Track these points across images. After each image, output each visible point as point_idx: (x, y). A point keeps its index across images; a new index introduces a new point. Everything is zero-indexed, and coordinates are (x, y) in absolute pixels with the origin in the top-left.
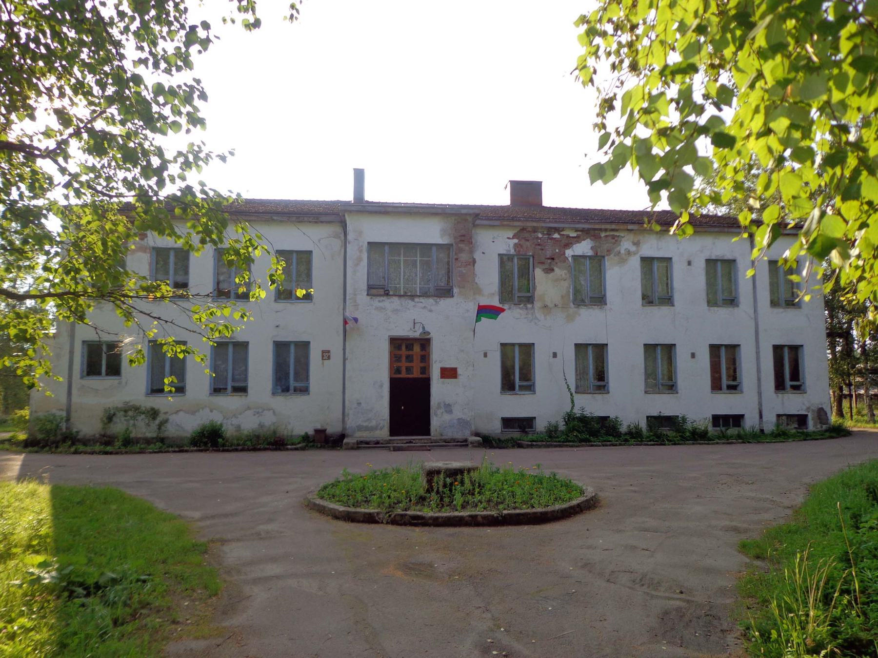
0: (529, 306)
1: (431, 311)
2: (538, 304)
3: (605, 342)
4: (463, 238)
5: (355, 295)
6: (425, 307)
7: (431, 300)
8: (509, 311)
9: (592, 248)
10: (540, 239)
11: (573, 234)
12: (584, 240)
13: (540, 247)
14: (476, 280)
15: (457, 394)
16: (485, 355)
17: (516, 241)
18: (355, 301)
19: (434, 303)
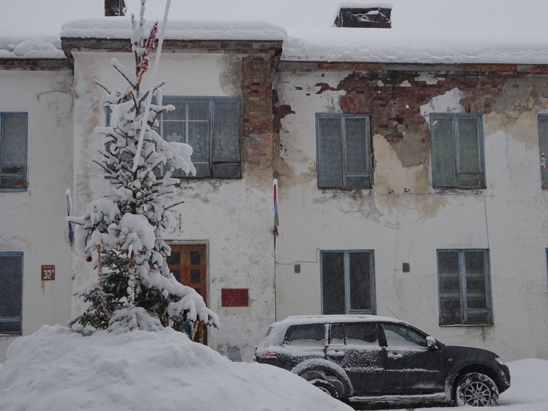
0: (365, 192)
1: (206, 201)
2: (377, 190)
3: (486, 247)
4: (255, 88)
5: (87, 177)
6: (197, 195)
7: (206, 185)
8: (334, 201)
9: (462, 102)
11: (431, 81)
12: (449, 89)
15: (248, 331)
16: (297, 269)
17: (343, 93)
18: (87, 187)
19: (211, 188)
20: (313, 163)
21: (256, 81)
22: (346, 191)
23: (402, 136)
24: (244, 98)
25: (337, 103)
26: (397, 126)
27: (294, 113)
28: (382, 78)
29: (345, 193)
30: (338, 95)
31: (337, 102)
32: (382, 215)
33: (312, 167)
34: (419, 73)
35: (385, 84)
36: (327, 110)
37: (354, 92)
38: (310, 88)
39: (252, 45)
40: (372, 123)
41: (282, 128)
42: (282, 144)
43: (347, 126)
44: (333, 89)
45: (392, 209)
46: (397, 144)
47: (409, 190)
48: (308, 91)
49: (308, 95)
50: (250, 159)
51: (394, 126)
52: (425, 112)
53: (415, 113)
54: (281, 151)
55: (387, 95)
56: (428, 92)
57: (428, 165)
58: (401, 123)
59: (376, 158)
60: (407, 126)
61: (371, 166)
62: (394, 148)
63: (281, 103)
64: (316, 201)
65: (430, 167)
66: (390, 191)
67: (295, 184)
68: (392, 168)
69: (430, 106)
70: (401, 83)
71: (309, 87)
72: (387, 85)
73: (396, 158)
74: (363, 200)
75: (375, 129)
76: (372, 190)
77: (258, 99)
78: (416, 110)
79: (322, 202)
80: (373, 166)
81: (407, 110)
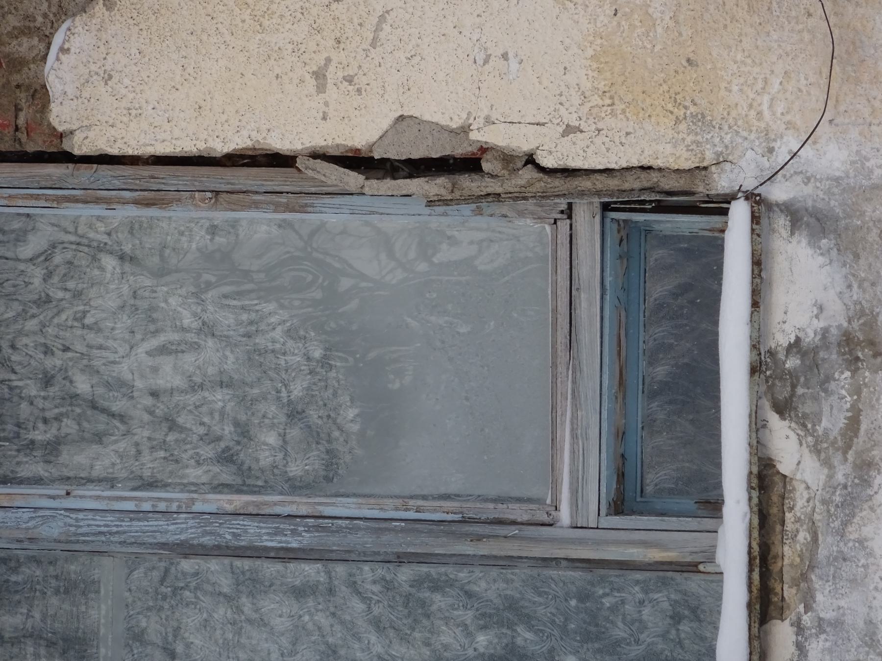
61: (469, 183)
76: (778, 193)
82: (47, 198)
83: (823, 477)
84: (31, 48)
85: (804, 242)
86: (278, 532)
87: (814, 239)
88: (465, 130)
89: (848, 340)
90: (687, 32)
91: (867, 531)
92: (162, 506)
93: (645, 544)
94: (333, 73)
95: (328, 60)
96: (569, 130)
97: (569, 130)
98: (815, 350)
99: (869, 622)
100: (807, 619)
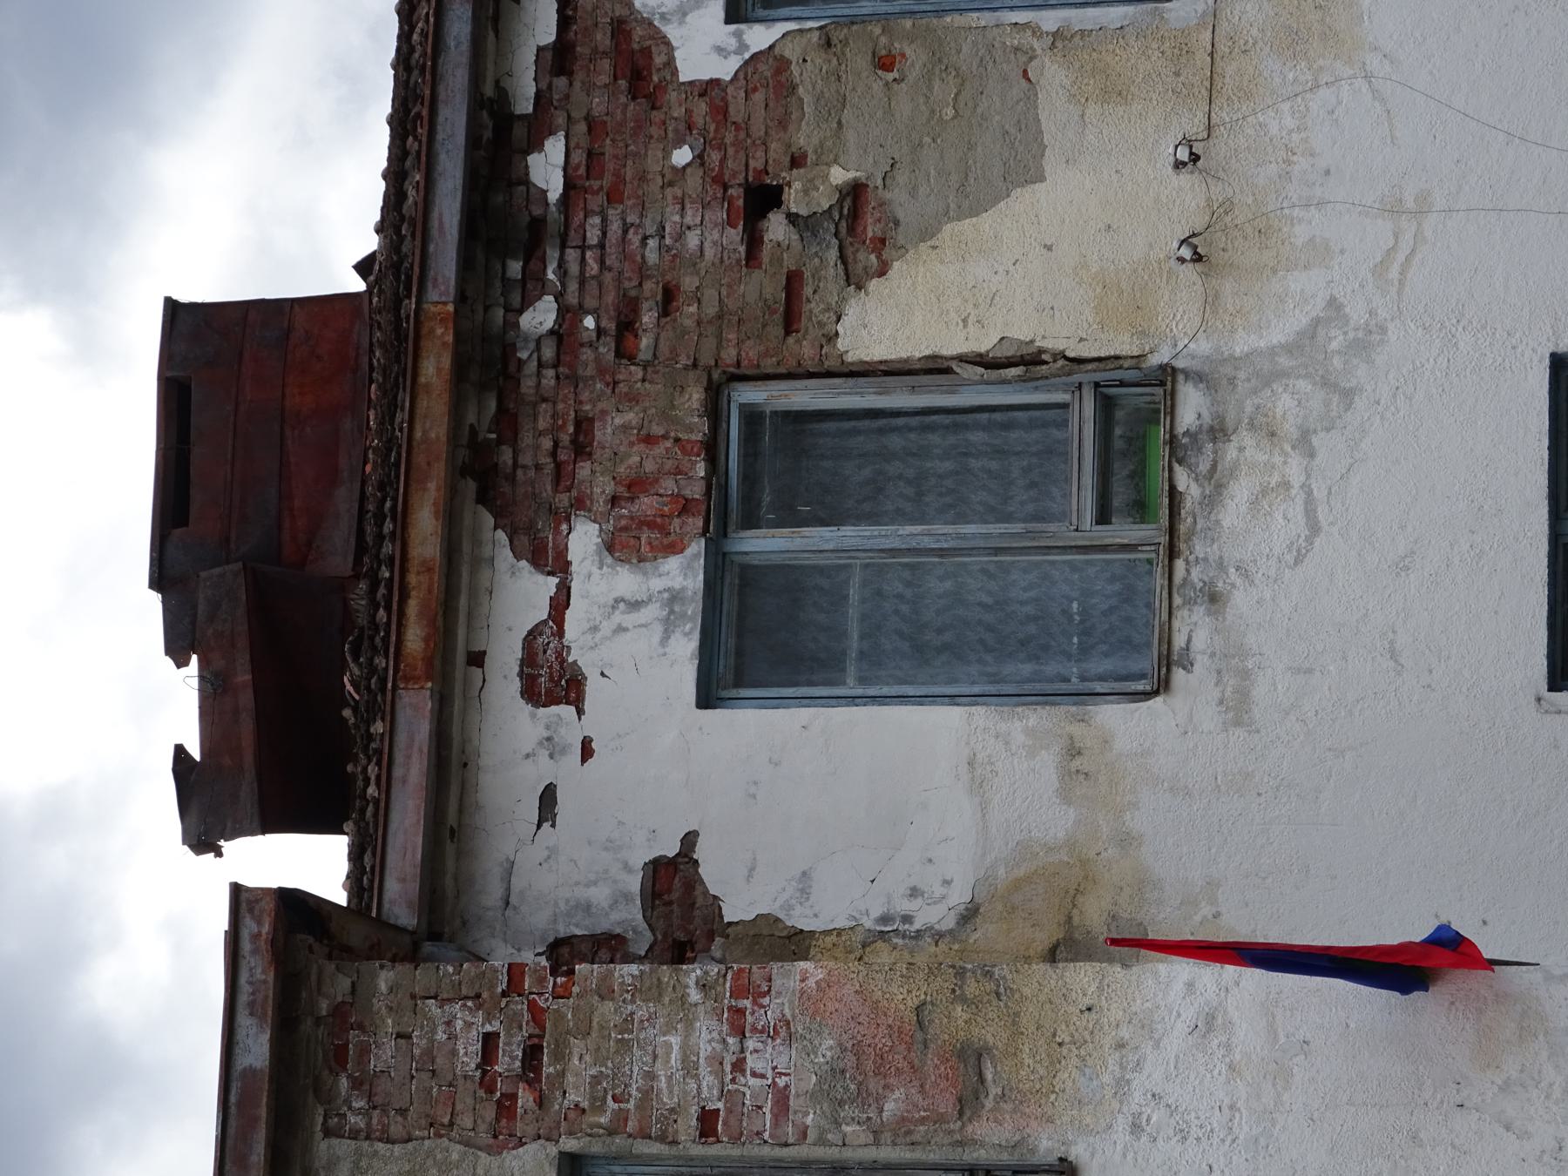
0: (1191, 408)
8: (1241, 601)
10: (568, 314)
13: (648, 318)
14: (934, 915)
17: (583, 539)
20: (1003, 727)
21: (468, 1055)
22: (1183, 528)
23: (855, 193)
24: (570, 1133)
25: (645, 574)
26: (792, 218)
27: (690, 840)
28: (507, 309)
29: (1192, 532)
30: (595, 570)
31: (639, 578)
32: (1333, 303)
33: (1029, 732)
34: (489, 90)
35: (543, 288)
36: (686, 634)
37: (584, 470)
38: (549, 739)
39: (250, 1072)
40: (770, 371)
41: (781, 916)
42: (876, 912)
43: (790, 518)
44: (560, 603)
45: (1299, 242)
46: (900, 215)
47: (1188, 142)
48: (564, 750)
49: (587, 751)
50: (947, 1105)
51: (795, 237)
52: (720, 50)
53: (721, 112)
54: (917, 925)
55: (608, 277)
56: (603, 39)
57: (1036, 31)
58: (779, 190)
59: (984, 342)
60: (797, 161)
62: (927, 233)
63: (630, 917)
64: (1238, 709)
65: (1050, 20)
66: (1186, 252)
67: (1127, 841)
68: (1049, 248)
69: (682, 22)
70: (544, 192)
71: (540, 743)
72: (551, 276)
73: (986, 221)
74: (1240, 422)
75: (807, 351)
77: (577, 1045)
78: (701, 108)
79: (1245, 674)
80: (1030, 361)
81: (700, 158)
82: (833, 393)
83: (1199, 492)
84: (829, 318)
85: (1191, 386)
86: (938, 541)
87: (1195, 386)
88: (1032, 342)
89: (1212, 429)
90: (1138, 295)
91: (1220, 517)
92: (883, 533)
93: (1112, 537)
94: (971, 320)
95: (969, 314)
96: (1081, 340)
97: (1081, 340)
98: (1196, 434)
99: (1221, 557)
100: (1192, 558)
